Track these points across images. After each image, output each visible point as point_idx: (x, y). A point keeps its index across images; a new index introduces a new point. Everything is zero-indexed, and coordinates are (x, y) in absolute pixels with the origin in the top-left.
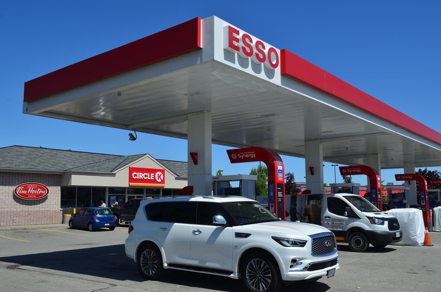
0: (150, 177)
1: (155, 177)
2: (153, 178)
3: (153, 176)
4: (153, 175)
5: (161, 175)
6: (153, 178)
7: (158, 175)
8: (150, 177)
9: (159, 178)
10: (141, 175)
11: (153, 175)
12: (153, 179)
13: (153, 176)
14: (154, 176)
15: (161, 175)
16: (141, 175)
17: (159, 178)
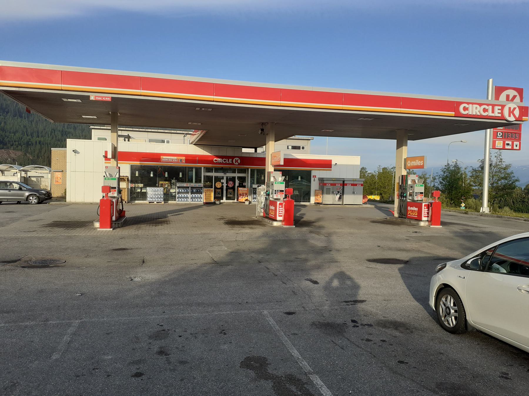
0: (493, 112)
1: (502, 113)
2: (499, 113)
3: (500, 111)
4: (499, 109)
5: (515, 109)
6: (499, 113)
7: (510, 108)
8: (493, 112)
9: (511, 115)
10: (476, 108)
11: (499, 109)
12: (500, 115)
13: (500, 111)
14: (502, 110)
15: (515, 109)
16: (476, 108)
17: (511, 115)
